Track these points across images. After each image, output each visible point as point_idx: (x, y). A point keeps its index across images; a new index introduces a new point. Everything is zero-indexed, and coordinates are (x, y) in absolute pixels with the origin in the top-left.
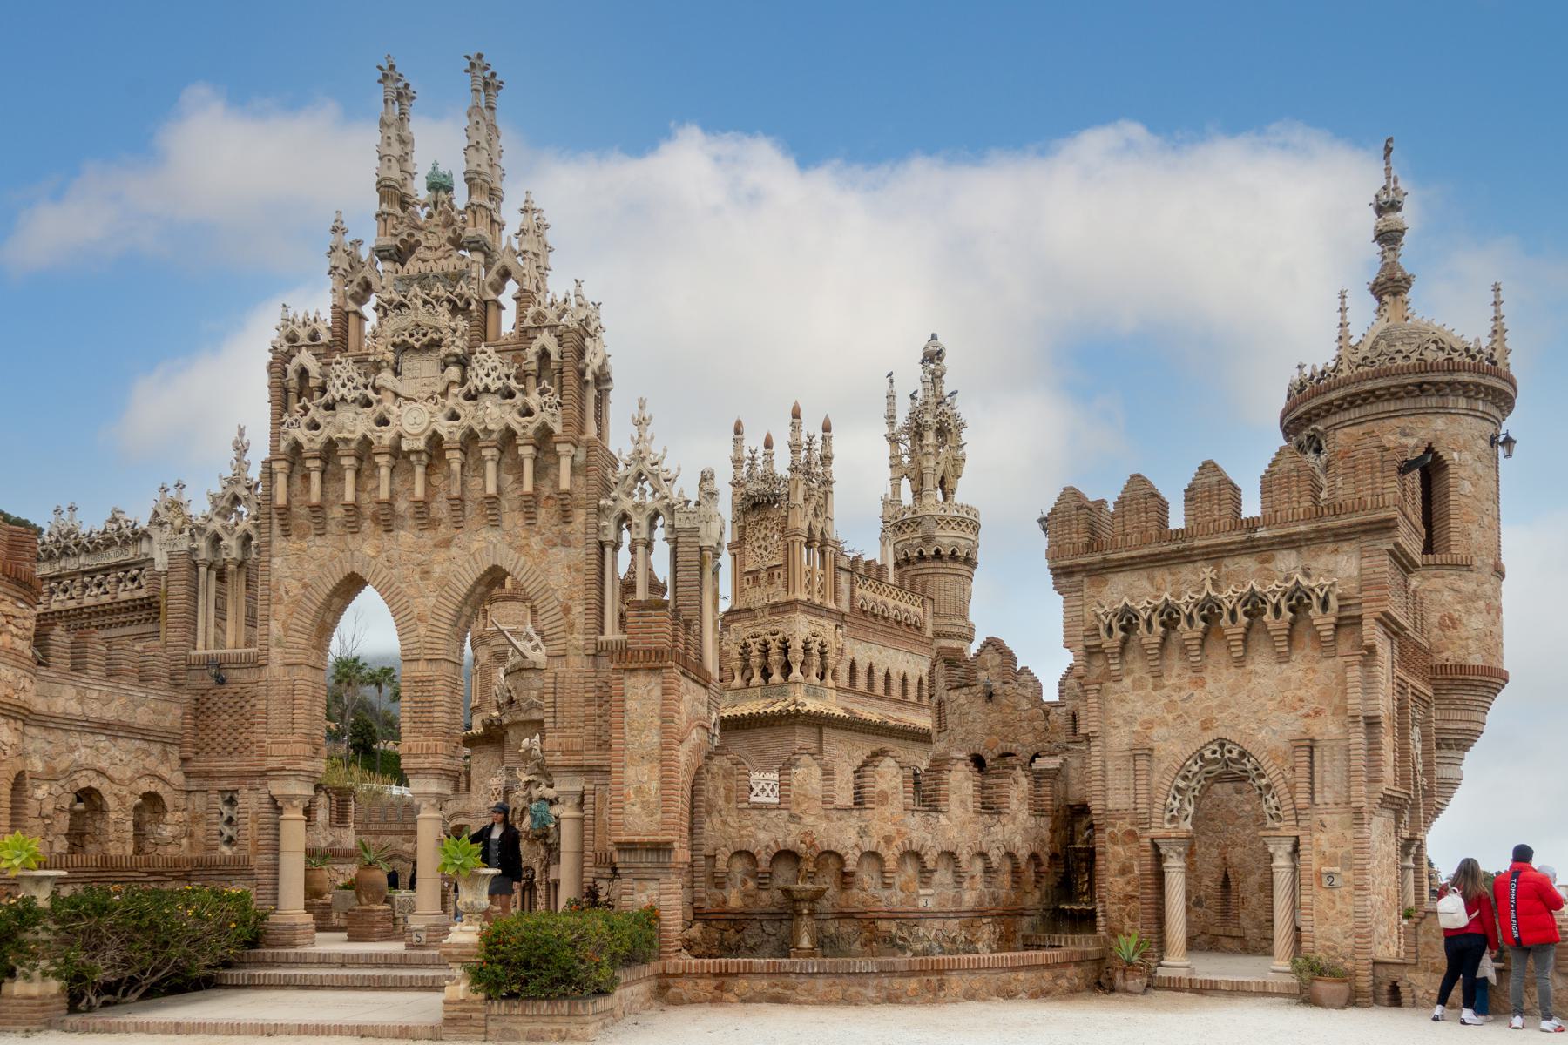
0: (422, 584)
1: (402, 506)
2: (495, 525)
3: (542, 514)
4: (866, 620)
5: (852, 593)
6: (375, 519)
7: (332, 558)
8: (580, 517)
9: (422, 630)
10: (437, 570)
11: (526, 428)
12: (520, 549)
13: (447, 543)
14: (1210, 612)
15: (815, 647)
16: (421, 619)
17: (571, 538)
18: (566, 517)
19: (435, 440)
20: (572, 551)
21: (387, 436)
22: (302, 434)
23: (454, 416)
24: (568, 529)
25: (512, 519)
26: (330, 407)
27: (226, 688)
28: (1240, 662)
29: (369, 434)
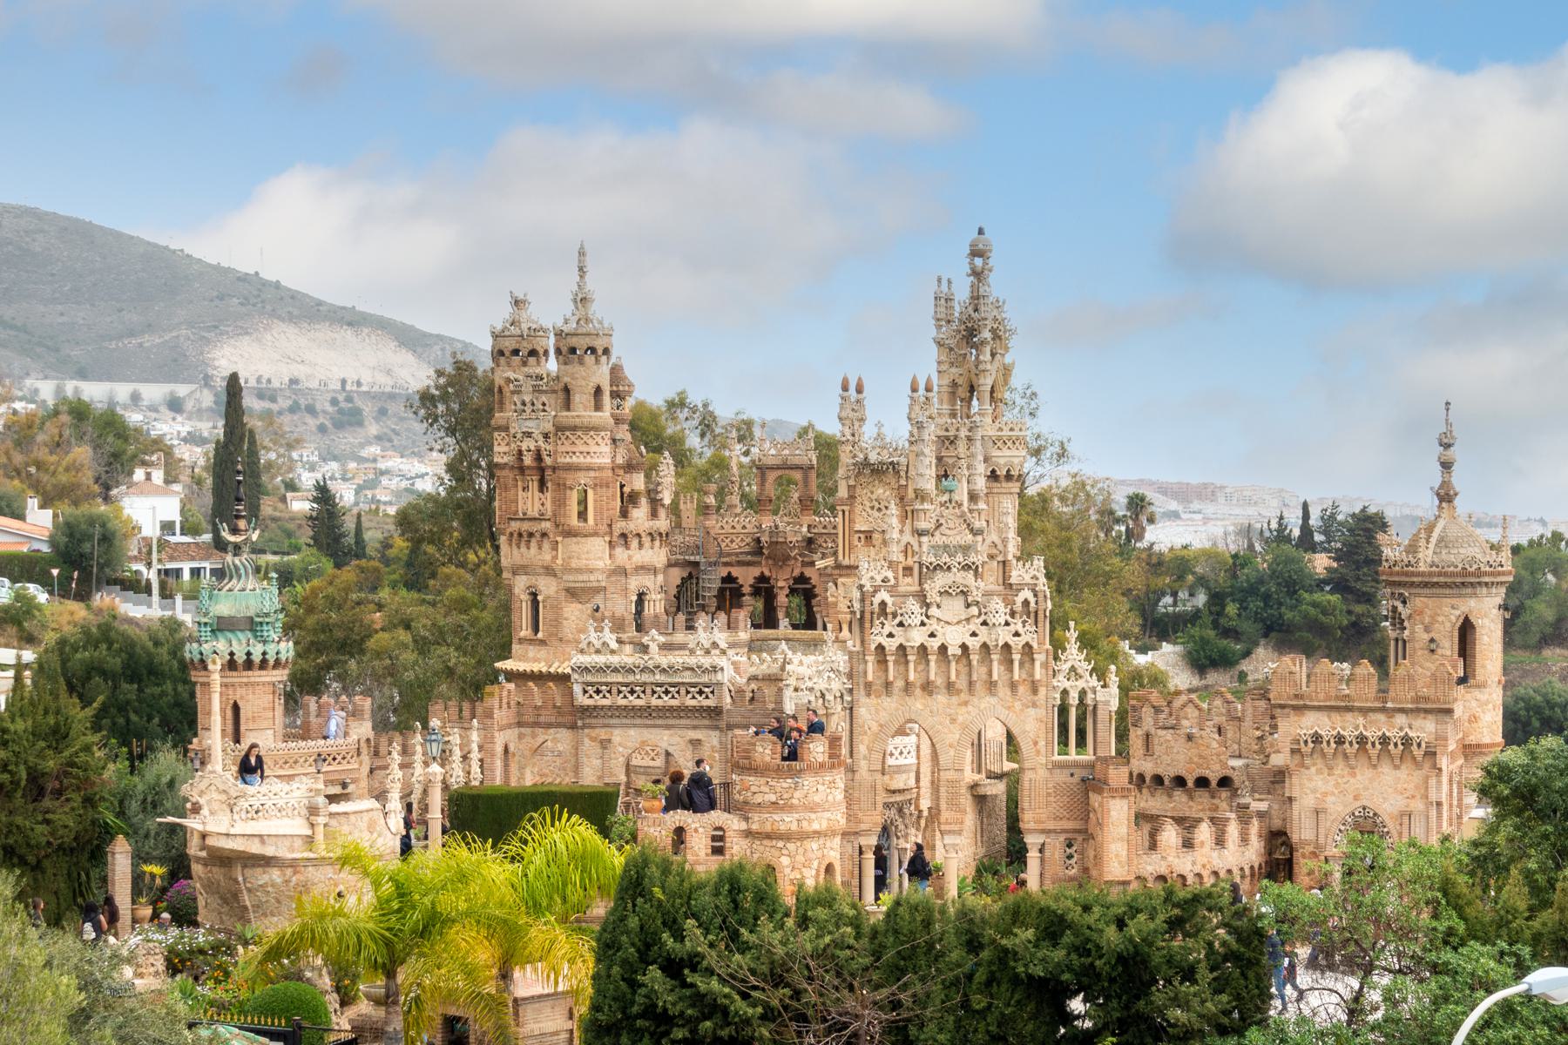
9: (952, 753)
10: (960, 719)
13: (966, 703)
14: (1362, 740)
18: (1035, 691)
23: (974, 634)
25: (1003, 691)
28: (1375, 766)
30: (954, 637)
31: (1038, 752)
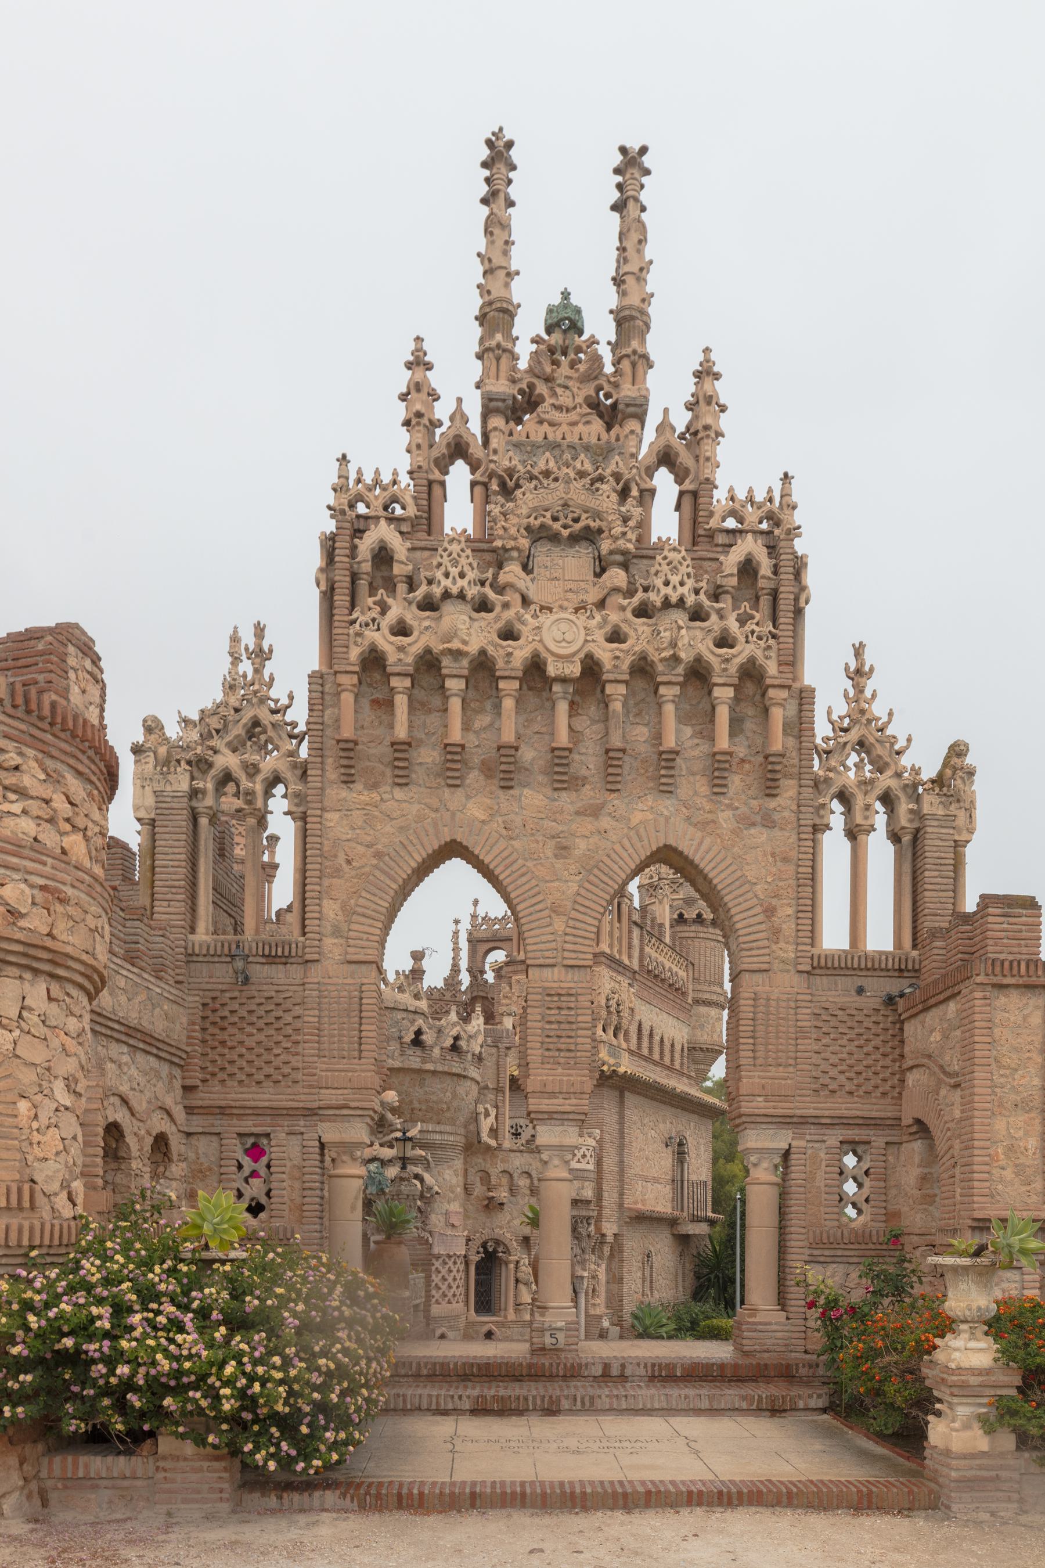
0: (559, 864)
1: (527, 754)
2: (666, 790)
3: (735, 782)
4: (651, 978)
5: (642, 950)
6: (487, 770)
7: (420, 819)
8: (789, 789)
9: (559, 924)
10: (581, 846)
11: (724, 666)
12: (702, 825)
13: (594, 811)
15: (613, 1003)
16: (555, 910)
17: (776, 816)
18: (770, 789)
19: (591, 668)
20: (777, 833)
21: (520, 653)
22: (384, 641)
24: (772, 803)
25: (693, 786)
26: (429, 605)
27: (252, 990)
29: (491, 650)
30: (563, 636)
31: (776, 934)
